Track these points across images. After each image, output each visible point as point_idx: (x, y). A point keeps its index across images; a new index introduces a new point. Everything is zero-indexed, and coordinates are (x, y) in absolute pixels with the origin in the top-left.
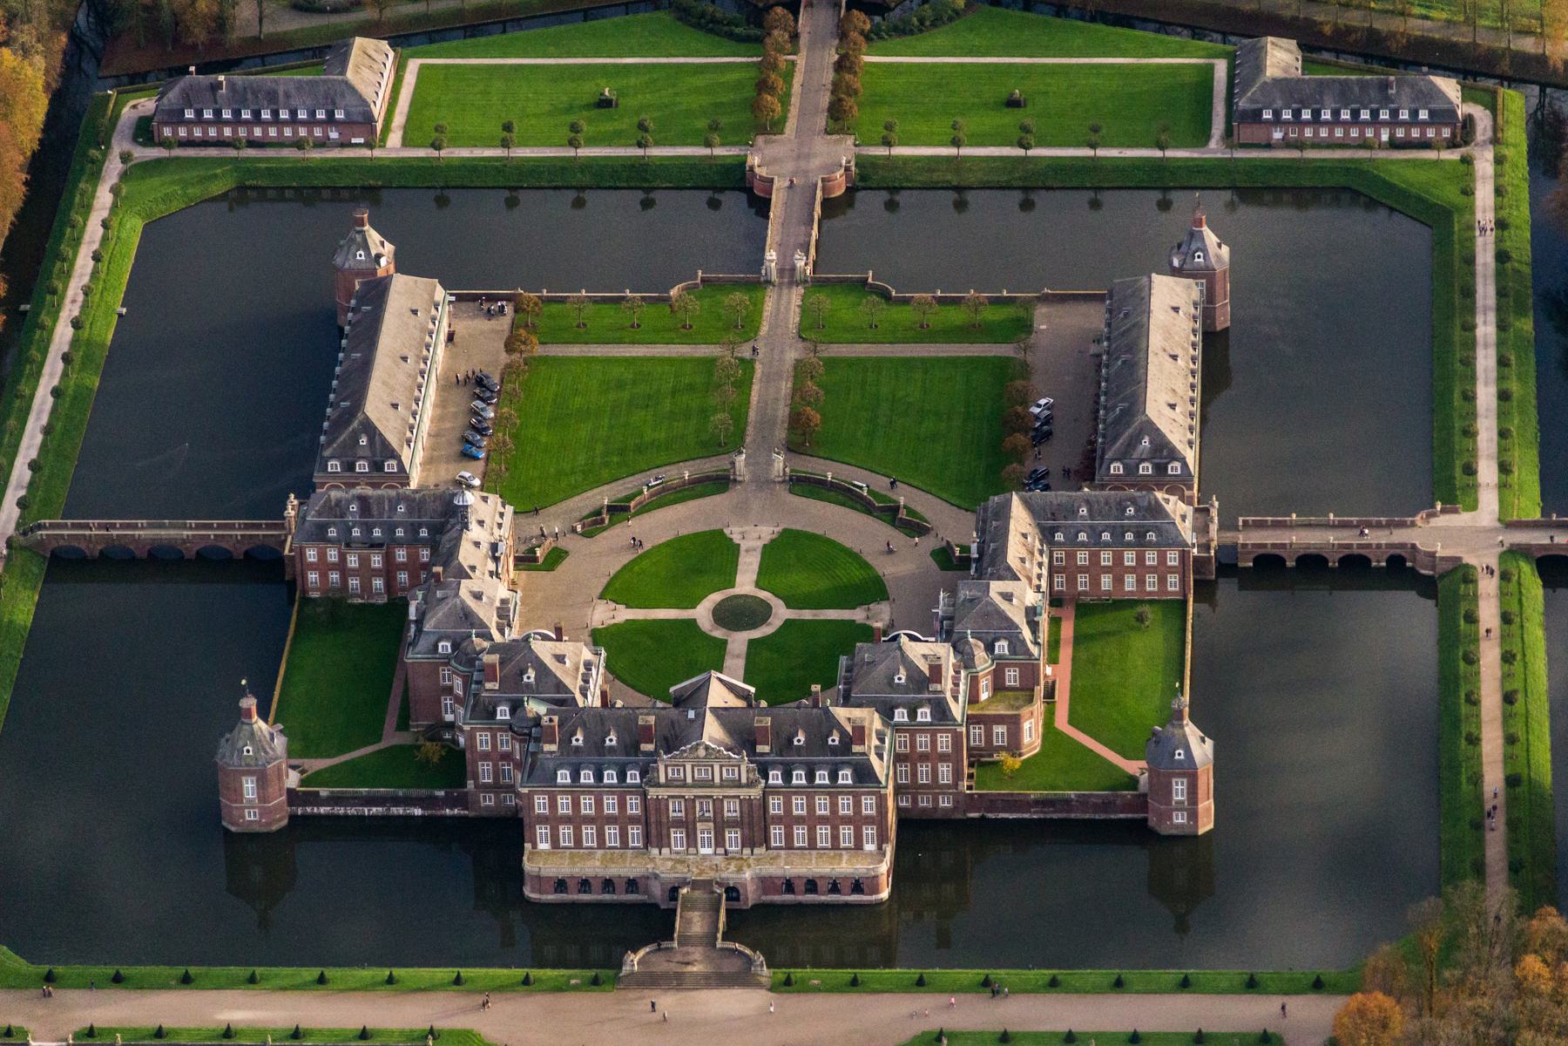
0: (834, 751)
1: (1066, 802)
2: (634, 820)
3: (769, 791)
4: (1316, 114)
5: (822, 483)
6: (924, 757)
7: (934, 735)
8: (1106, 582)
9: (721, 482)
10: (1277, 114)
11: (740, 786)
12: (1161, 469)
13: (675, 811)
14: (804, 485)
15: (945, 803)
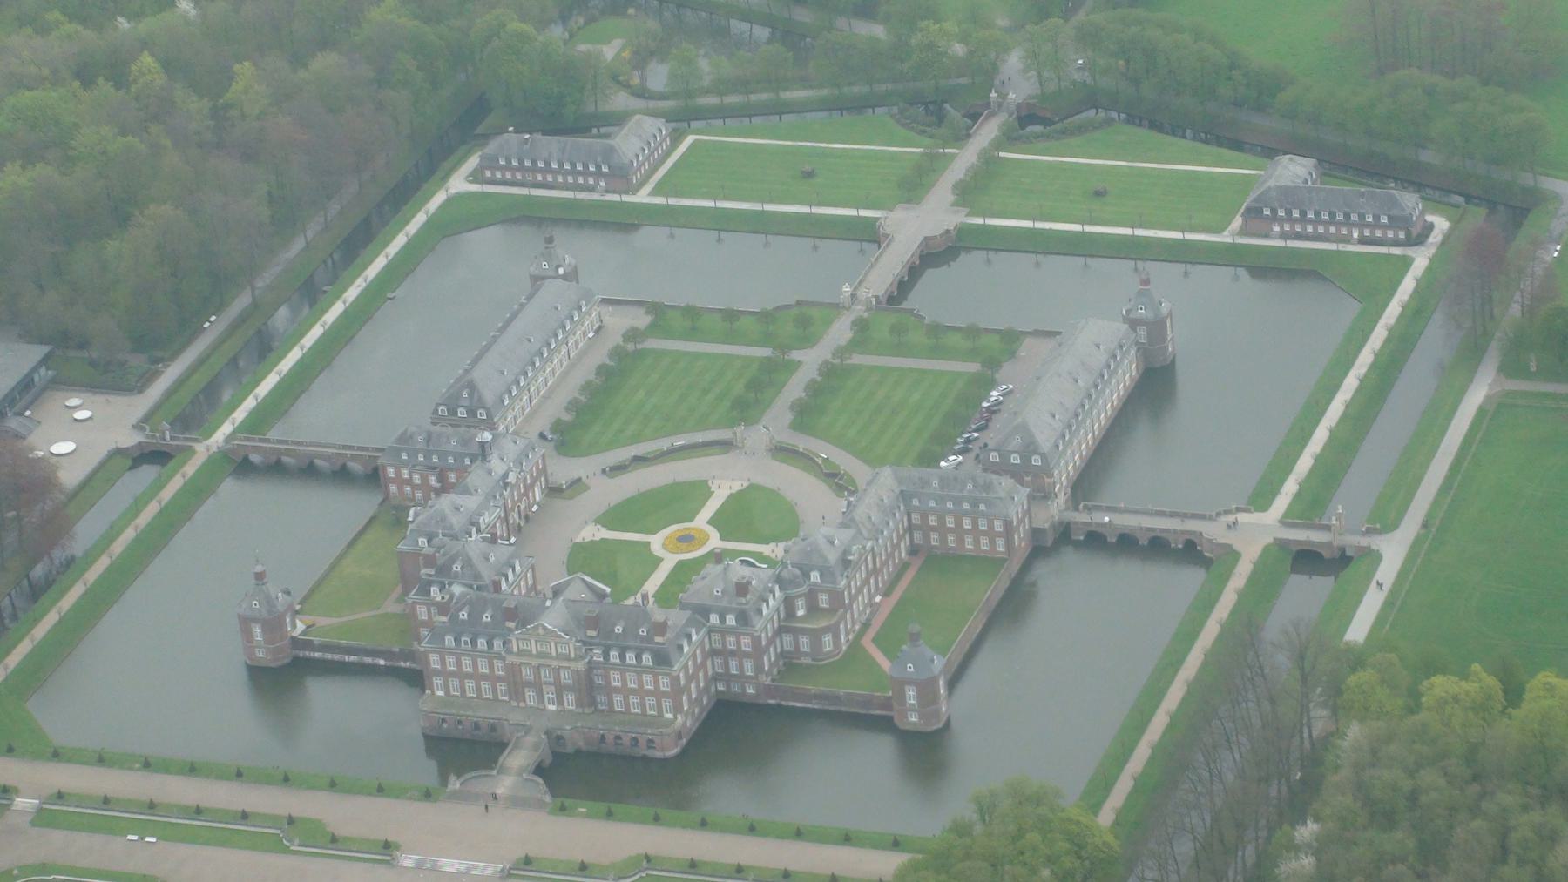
0: (643, 639)
1: (837, 699)
2: (500, 679)
3: (591, 666)
4: (1303, 213)
5: (796, 452)
6: (733, 653)
7: (738, 636)
8: (951, 540)
9: (726, 446)
10: (1274, 211)
11: (568, 659)
12: (1026, 459)
13: (527, 674)
14: (782, 452)
15: (750, 690)
